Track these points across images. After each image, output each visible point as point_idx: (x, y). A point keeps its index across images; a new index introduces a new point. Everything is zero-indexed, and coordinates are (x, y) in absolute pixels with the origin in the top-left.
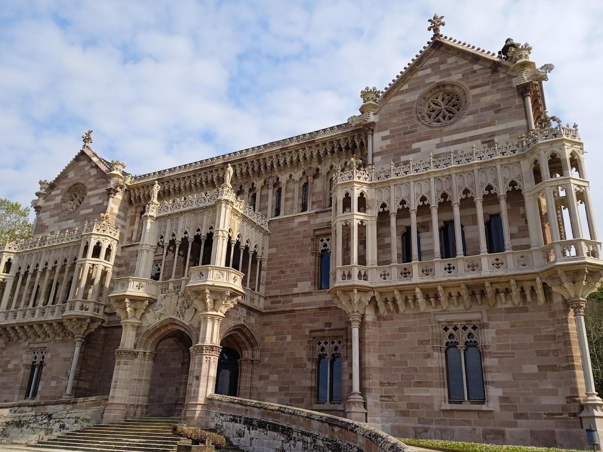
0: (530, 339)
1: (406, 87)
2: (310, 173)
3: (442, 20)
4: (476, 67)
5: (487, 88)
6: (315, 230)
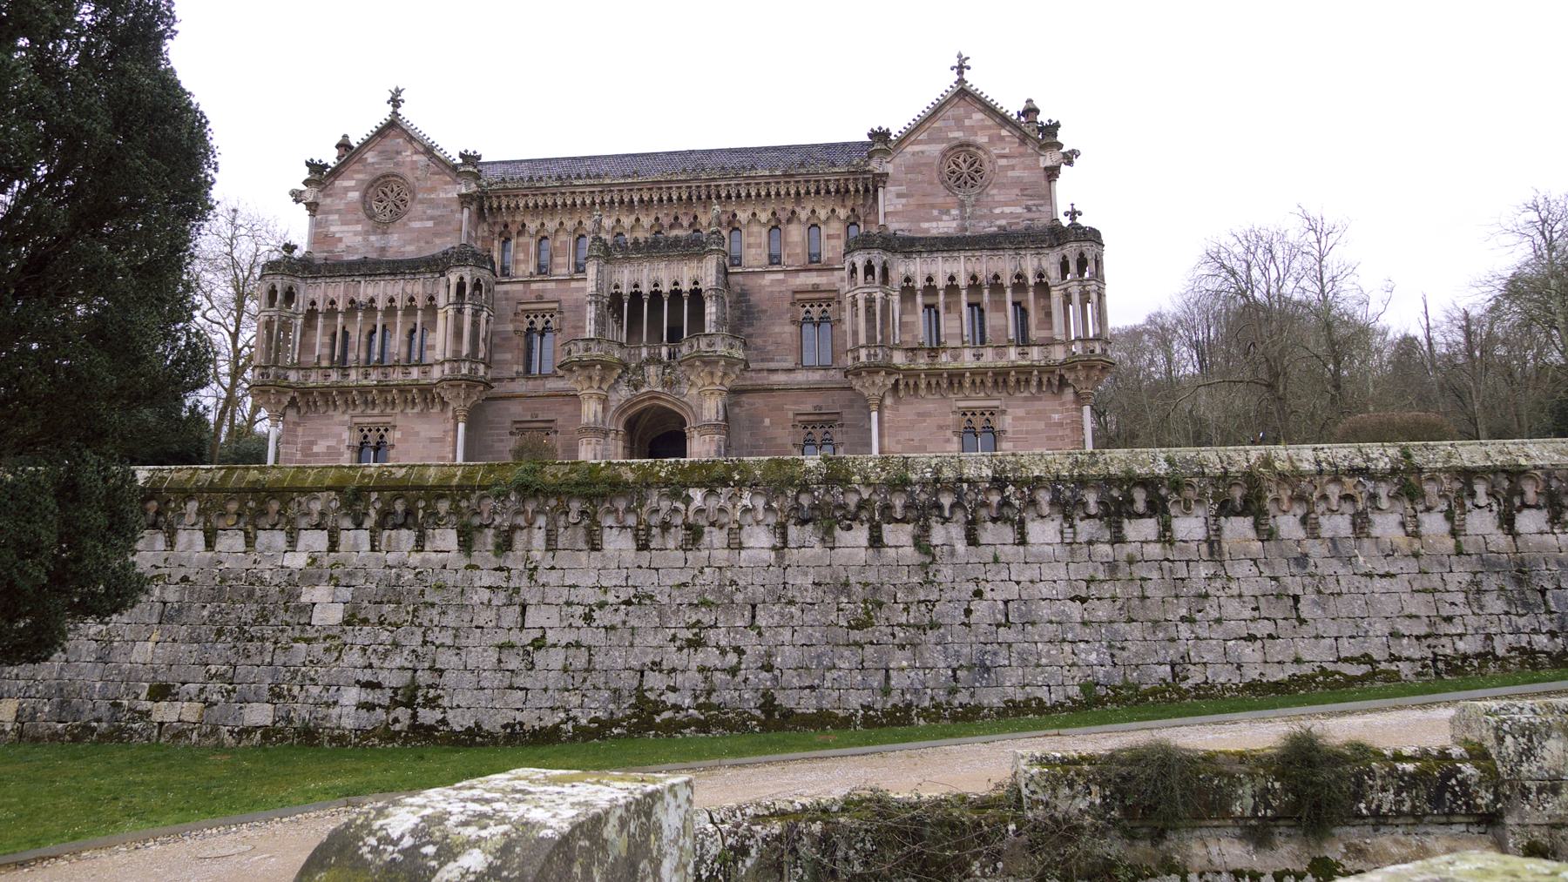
0: (1041, 425)
1: (923, 136)
2: (783, 216)
3: (967, 63)
4: (1004, 133)
5: (1013, 162)
6: (795, 292)
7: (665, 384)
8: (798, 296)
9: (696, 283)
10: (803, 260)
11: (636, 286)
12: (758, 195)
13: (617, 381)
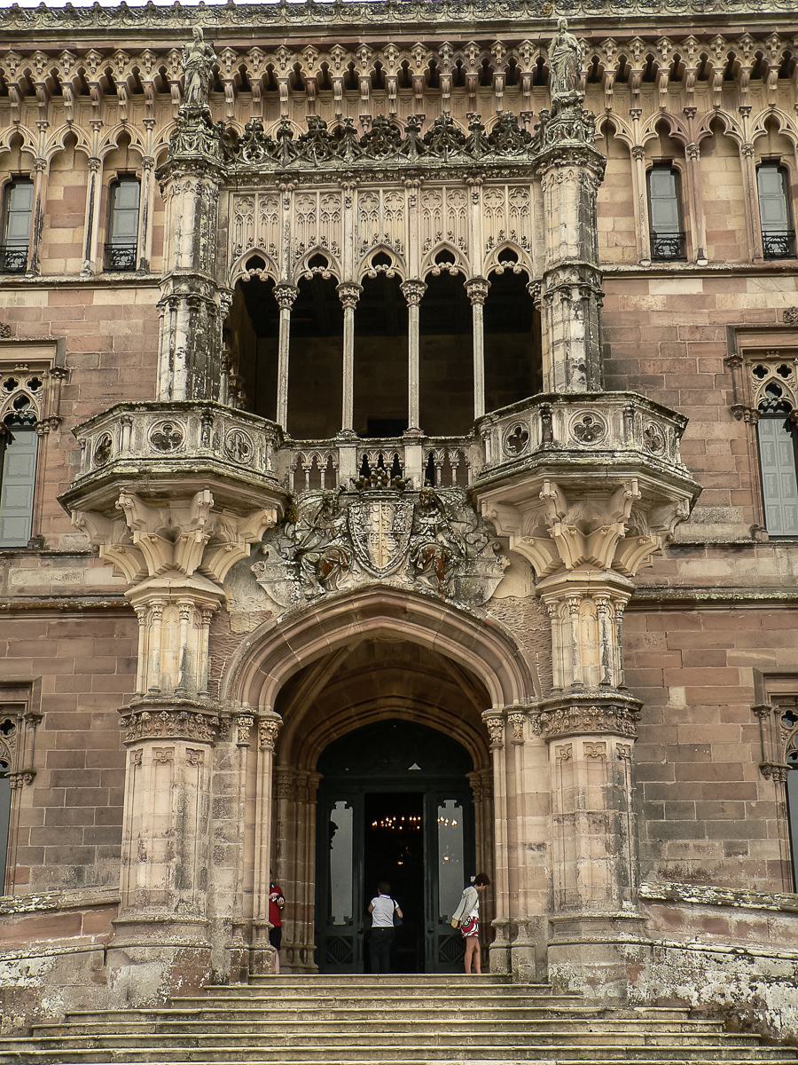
7: (420, 562)
8: (747, 341)
9: (508, 255)
10: (747, 252)
11: (318, 260)
12: (623, 75)
13: (258, 552)
